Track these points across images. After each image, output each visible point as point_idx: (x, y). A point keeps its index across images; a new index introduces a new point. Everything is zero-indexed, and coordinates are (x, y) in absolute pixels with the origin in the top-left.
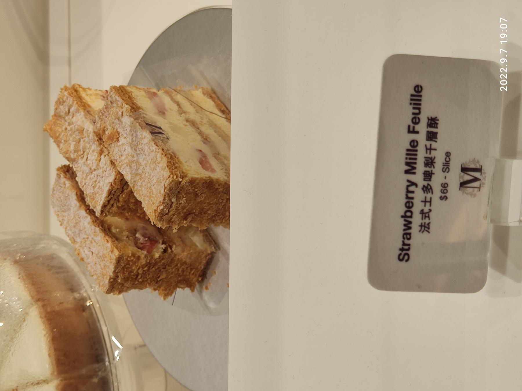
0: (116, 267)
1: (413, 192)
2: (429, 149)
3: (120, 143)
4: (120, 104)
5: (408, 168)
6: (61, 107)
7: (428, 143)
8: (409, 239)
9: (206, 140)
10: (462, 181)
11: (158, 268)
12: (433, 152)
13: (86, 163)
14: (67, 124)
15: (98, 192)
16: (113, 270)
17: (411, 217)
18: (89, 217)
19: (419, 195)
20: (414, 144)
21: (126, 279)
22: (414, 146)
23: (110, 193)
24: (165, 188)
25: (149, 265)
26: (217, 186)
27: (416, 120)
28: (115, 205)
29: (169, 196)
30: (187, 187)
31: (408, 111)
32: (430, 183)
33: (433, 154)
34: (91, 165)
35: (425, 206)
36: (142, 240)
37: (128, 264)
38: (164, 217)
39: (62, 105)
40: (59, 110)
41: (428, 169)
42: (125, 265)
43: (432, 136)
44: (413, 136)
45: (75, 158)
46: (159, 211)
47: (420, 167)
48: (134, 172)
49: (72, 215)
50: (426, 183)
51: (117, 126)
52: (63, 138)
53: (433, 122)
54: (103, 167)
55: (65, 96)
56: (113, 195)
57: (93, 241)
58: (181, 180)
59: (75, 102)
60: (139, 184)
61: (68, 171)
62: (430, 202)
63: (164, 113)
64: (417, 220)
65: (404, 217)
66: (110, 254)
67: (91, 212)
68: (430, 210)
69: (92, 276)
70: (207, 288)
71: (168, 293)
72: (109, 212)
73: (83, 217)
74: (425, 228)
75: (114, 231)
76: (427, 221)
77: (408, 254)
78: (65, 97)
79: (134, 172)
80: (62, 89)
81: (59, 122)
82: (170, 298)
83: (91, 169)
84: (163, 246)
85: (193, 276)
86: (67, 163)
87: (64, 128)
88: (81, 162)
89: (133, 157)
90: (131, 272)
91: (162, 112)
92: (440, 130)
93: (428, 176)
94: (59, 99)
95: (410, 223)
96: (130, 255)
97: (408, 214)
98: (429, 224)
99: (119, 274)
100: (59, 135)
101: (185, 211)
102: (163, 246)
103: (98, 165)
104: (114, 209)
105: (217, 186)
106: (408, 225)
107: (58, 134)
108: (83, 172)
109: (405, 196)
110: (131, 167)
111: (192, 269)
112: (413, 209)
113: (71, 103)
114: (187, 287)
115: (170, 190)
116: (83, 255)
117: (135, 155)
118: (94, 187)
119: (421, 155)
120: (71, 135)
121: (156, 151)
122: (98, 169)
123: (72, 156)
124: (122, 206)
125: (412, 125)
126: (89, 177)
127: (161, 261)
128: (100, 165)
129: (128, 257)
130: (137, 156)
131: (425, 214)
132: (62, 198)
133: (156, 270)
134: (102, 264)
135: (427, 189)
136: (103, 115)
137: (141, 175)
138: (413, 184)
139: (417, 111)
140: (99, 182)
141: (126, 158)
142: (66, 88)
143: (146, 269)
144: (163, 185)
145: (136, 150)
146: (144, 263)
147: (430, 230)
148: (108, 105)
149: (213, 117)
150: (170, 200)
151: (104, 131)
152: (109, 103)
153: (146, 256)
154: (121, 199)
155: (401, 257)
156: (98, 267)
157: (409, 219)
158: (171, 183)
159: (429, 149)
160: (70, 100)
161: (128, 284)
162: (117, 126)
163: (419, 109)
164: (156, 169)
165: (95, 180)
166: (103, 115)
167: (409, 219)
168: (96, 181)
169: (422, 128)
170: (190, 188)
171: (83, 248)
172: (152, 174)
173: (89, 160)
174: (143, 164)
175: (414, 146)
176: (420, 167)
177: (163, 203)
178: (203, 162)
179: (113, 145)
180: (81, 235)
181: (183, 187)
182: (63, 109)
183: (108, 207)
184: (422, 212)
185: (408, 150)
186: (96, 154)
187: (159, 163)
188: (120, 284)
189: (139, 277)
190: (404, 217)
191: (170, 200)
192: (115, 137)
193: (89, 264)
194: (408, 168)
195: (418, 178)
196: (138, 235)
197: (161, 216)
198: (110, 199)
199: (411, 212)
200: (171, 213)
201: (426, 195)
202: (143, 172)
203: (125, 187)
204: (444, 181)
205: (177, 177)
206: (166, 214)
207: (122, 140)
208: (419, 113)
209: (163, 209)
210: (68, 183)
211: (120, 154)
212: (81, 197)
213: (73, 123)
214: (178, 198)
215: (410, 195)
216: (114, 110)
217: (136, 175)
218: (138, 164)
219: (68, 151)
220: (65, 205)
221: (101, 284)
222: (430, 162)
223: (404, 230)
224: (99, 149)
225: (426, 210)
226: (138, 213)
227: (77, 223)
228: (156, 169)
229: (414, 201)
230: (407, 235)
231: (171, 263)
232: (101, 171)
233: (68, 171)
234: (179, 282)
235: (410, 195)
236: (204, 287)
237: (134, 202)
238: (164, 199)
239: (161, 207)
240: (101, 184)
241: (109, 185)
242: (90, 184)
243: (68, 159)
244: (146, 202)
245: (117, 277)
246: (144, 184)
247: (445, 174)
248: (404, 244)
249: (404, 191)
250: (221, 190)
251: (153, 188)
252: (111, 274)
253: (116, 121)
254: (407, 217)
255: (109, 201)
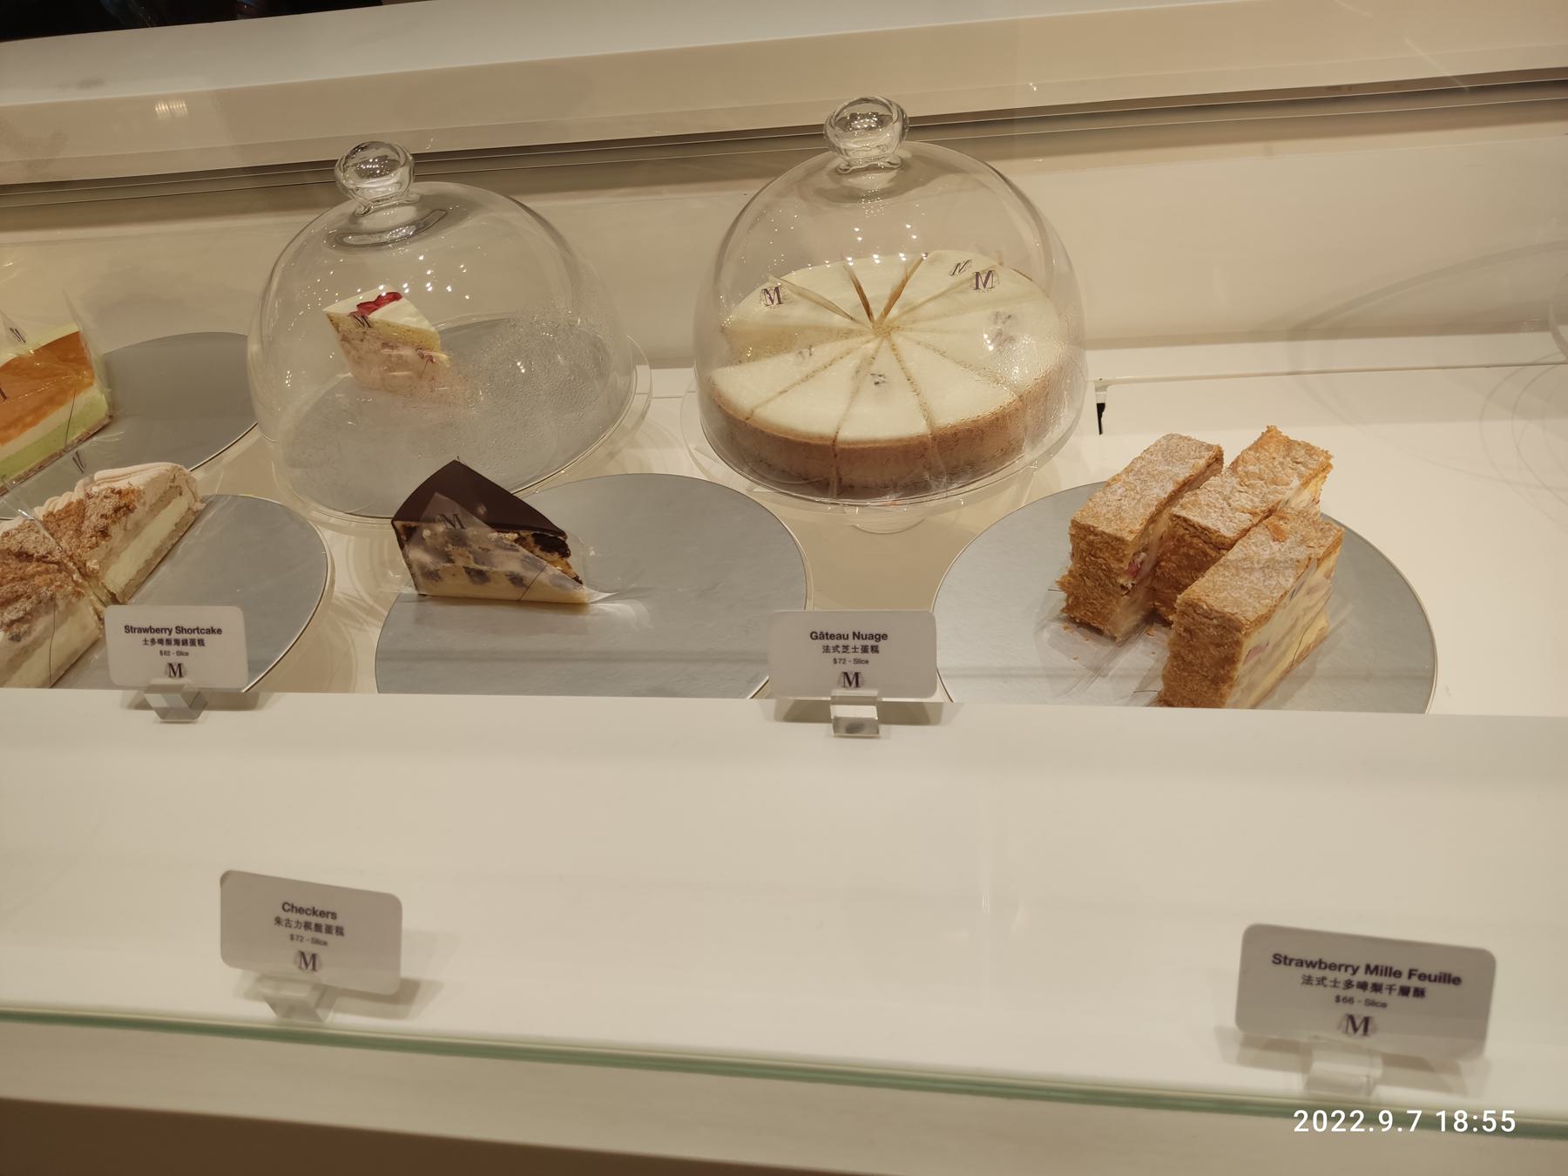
0: (1109, 535)
1: (1346, 970)
2: (1391, 988)
3: (1272, 544)
4: (1322, 542)
5: (1372, 967)
6: (1303, 452)
7: (1397, 988)
8: (1296, 965)
9: (1277, 645)
10: (1355, 1017)
11: (1101, 579)
12: (1388, 991)
13: (1235, 490)
14: (1282, 460)
15: (1203, 511)
16: (1107, 531)
17: (1320, 968)
18: (1166, 496)
19: (1343, 976)
20: (1398, 974)
21: (1091, 544)
22: (1395, 974)
23: (1205, 529)
24: (1233, 615)
25: (1110, 570)
26: (1227, 668)
27: (1422, 977)
28: (1188, 532)
29: (1221, 617)
30: (1232, 638)
31: (1434, 970)
32: (1355, 987)
33: (1386, 992)
34: (1233, 498)
35: (1331, 981)
36: (1139, 560)
37: (1113, 548)
38: (1191, 608)
39: (1306, 453)
40: (1298, 449)
41: (1370, 986)
42: (1112, 546)
43: (1404, 991)
44: (1405, 974)
45: (1237, 473)
46: (1201, 603)
47: (1372, 979)
48: (1239, 564)
49: (1161, 468)
50: (1355, 983)
51: (1293, 539)
52: (1263, 454)
53: (1419, 993)
54: (1235, 517)
55: (1319, 457)
56: (1202, 532)
57: (1136, 501)
58: (1243, 633)
59: (1311, 472)
60: (1227, 574)
61: (1217, 459)
62: (1335, 986)
63: (1308, 594)
64: (1316, 973)
65: (1321, 962)
66: (1128, 529)
67: (1173, 498)
68: (1325, 986)
69: (1090, 500)
70: (1066, 628)
71: (1064, 586)
72: (1177, 524)
73: (1162, 486)
74: (1308, 980)
75: (1151, 527)
76: (1315, 982)
77: (1280, 962)
78: (1317, 458)
79: (1239, 564)
80: (1329, 457)
81: (1282, 446)
82: (1057, 587)
83: (1230, 498)
84: (1130, 586)
85: (1082, 613)
86: (1227, 461)
87: (1274, 455)
88: (1235, 481)
89: (1258, 563)
90: (1101, 550)
91: (1310, 592)
92: (1411, 1000)
93: (1363, 986)
94: (1313, 448)
95: (1314, 967)
96: (1126, 552)
97: (1323, 966)
98: (1311, 984)
99: (1100, 537)
100: (1265, 450)
101: (1198, 631)
102: (1130, 586)
103: (1237, 510)
104: (1181, 531)
105: (1227, 668)
106: (1311, 964)
107: (1266, 447)
108: (1222, 486)
109: (1342, 963)
110: (1245, 559)
111: (1093, 613)
112: (1327, 970)
113: (1310, 466)
114: (1068, 605)
115: (1230, 620)
116: (1115, 487)
117: (1261, 565)
118: (1208, 505)
119: (1385, 980)
120: (1267, 466)
121: (1273, 597)
122: (1231, 509)
123: (1239, 469)
124: (1184, 540)
125: (1418, 973)
126: (1218, 495)
127: (1112, 583)
128: (1237, 513)
129: (1123, 550)
130: (1261, 568)
131: (1322, 981)
132: (1181, 453)
133: (1100, 576)
134: (1110, 515)
135: (1349, 984)
136: (1304, 517)
137: (1237, 575)
138: (1355, 971)
139: (1433, 978)
140: (1215, 512)
141: (1255, 553)
142: (1329, 457)
143: (1104, 567)
144: (1235, 611)
145: (1268, 567)
146: (1112, 566)
147: (1304, 985)
148: (1319, 525)
149: (1296, 645)
150: (1215, 618)
151: (1282, 518)
152: (1321, 527)
153: (1122, 568)
154: (1195, 540)
155: (1278, 957)
156: (1104, 511)
157: (1317, 966)
158: (1240, 622)
159: (1391, 988)
160: (1313, 465)
161: (1083, 545)
162: (1293, 539)
163: (1435, 980)
164: (1250, 598)
165: (1218, 505)
166: (1304, 517)
167: (1317, 966)
168: (1215, 506)
169: (1415, 983)
170: (1230, 640)
171: (1124, 487)
172: (1242, 592)
173: (1240, 496)
174: (1253, 578)
175: (1395, 974)
176: (1372, 979)
177: (1211, 610)
178: (1257, 649)
179: (1268, 533)
180: (1139, 482)
181: (1231, 632)
182: (1300, 454)
183: (1184, 524)
184: (1324, 979)
185: (1391, 969)
186: (1249, 506)
187: (1259, 602)
188: (1085, 536)
189: (1092, 558)
190: (1321, 962)
191: (1215, 618)
192: (1278, 536)
193: (1105, 494)
194: (1372, 967)
195: (1361, 976)
196: (1143, 554)
197: (1193, 606)
198: (1195, 528)
199: (1325, 968)
200: (1195, 615)
201: (1342, 982)
202: (1242, 578)
203: (1212, 546)
204: (1355, 1000)
205: (1247, 629)
206: (1195, 611)
207: (1276, 546)
208: (1430, 980)
209: (1202, 608)
210: (1202, 463)
211: (1259, 543)
212: (1190, 484)
213: (1283, 469)
214: (1216, 627)
215: (1343, 969)
216: (1313, 534)
217: (1237, 568)
218: (1251, 570)
219: (1246, 463)
220: (1172, 457)
221: (1084, 514)
222: (1377, 988)
223: (1306, 961)
224: (1258, 510)
225: (1326, 982)
226: (1171, 555)
227: (1154, 476)
228: (1250, 598)
229: (1336, 972)
230: (1300, 963)
231: (1106, 593)
232: (1230, 515)
233: (1217, 459)
234: (1076, 598)
235: (1343, 969)
236: (1067, 624)
237: (1189, 554)
238: (1217, 611)
239: (1205, 607)
240: (1214, 515)
241: (1215, 528)
242: (1211, 499)
243: (1235, 464)
244: (1207, 584)
245: (1096, 535)
246: (1227, 579)
247: (1363, 1002)
248: (1291, 960)
249: (1348, 963)
250: (1222, 672)
251: (1225, 593)
252: (1100, 529)
253: (1299, 538)
254: (1320, 964)
255: (1193, 526)
